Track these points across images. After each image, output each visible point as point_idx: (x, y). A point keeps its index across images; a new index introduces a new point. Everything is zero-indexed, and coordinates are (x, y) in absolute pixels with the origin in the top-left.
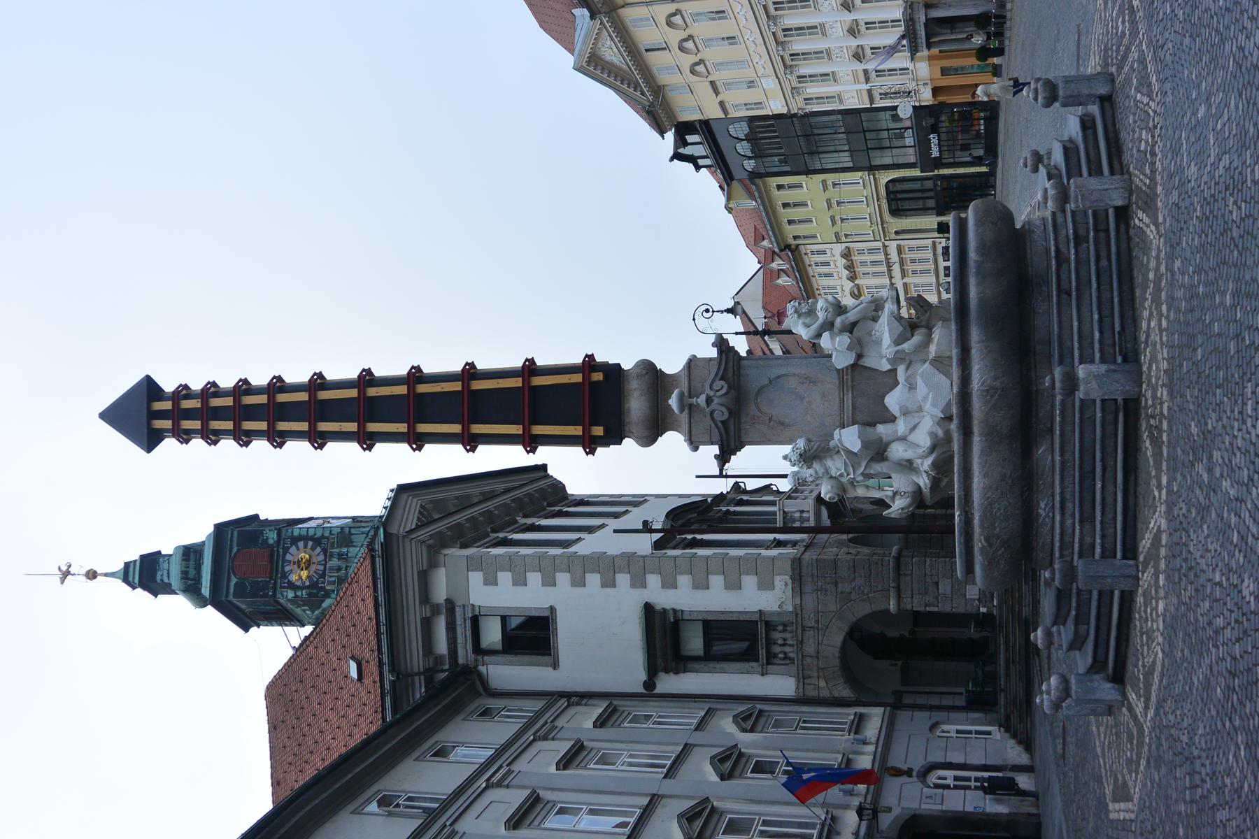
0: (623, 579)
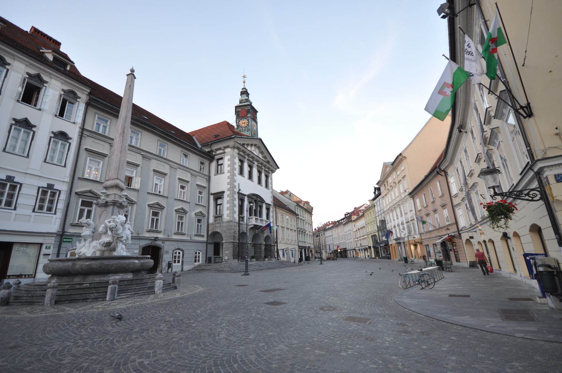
0: (229, 186)
